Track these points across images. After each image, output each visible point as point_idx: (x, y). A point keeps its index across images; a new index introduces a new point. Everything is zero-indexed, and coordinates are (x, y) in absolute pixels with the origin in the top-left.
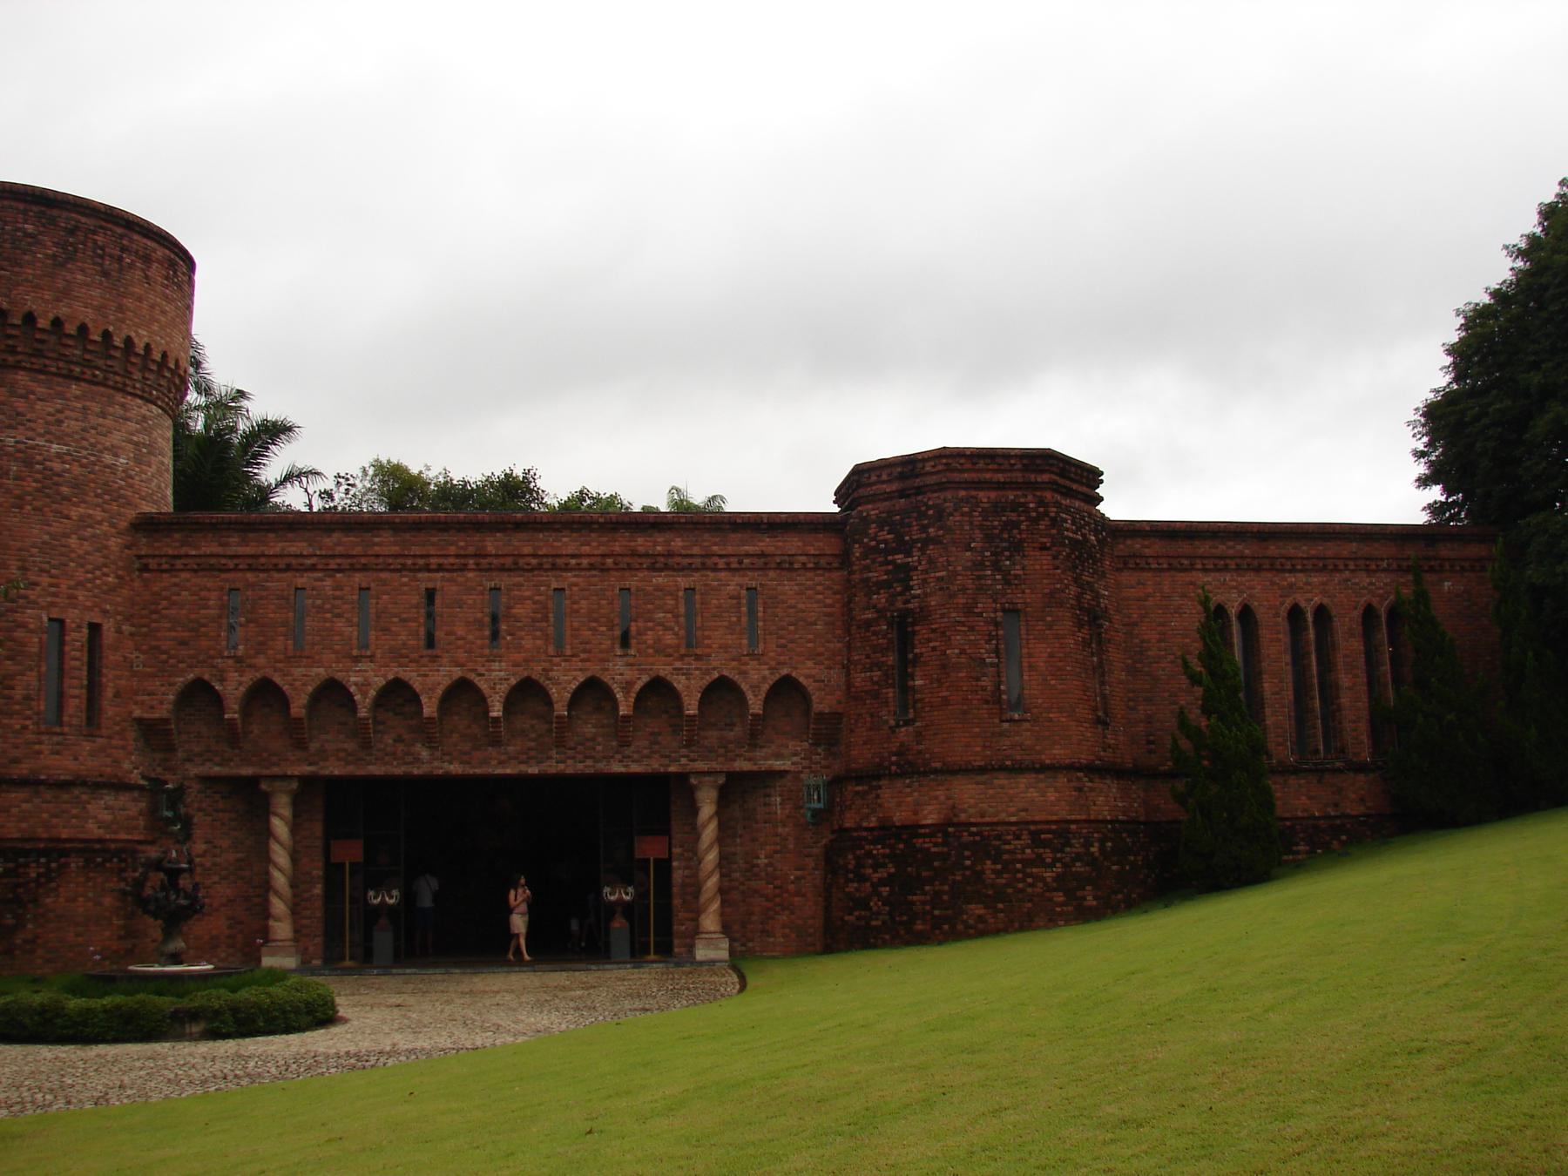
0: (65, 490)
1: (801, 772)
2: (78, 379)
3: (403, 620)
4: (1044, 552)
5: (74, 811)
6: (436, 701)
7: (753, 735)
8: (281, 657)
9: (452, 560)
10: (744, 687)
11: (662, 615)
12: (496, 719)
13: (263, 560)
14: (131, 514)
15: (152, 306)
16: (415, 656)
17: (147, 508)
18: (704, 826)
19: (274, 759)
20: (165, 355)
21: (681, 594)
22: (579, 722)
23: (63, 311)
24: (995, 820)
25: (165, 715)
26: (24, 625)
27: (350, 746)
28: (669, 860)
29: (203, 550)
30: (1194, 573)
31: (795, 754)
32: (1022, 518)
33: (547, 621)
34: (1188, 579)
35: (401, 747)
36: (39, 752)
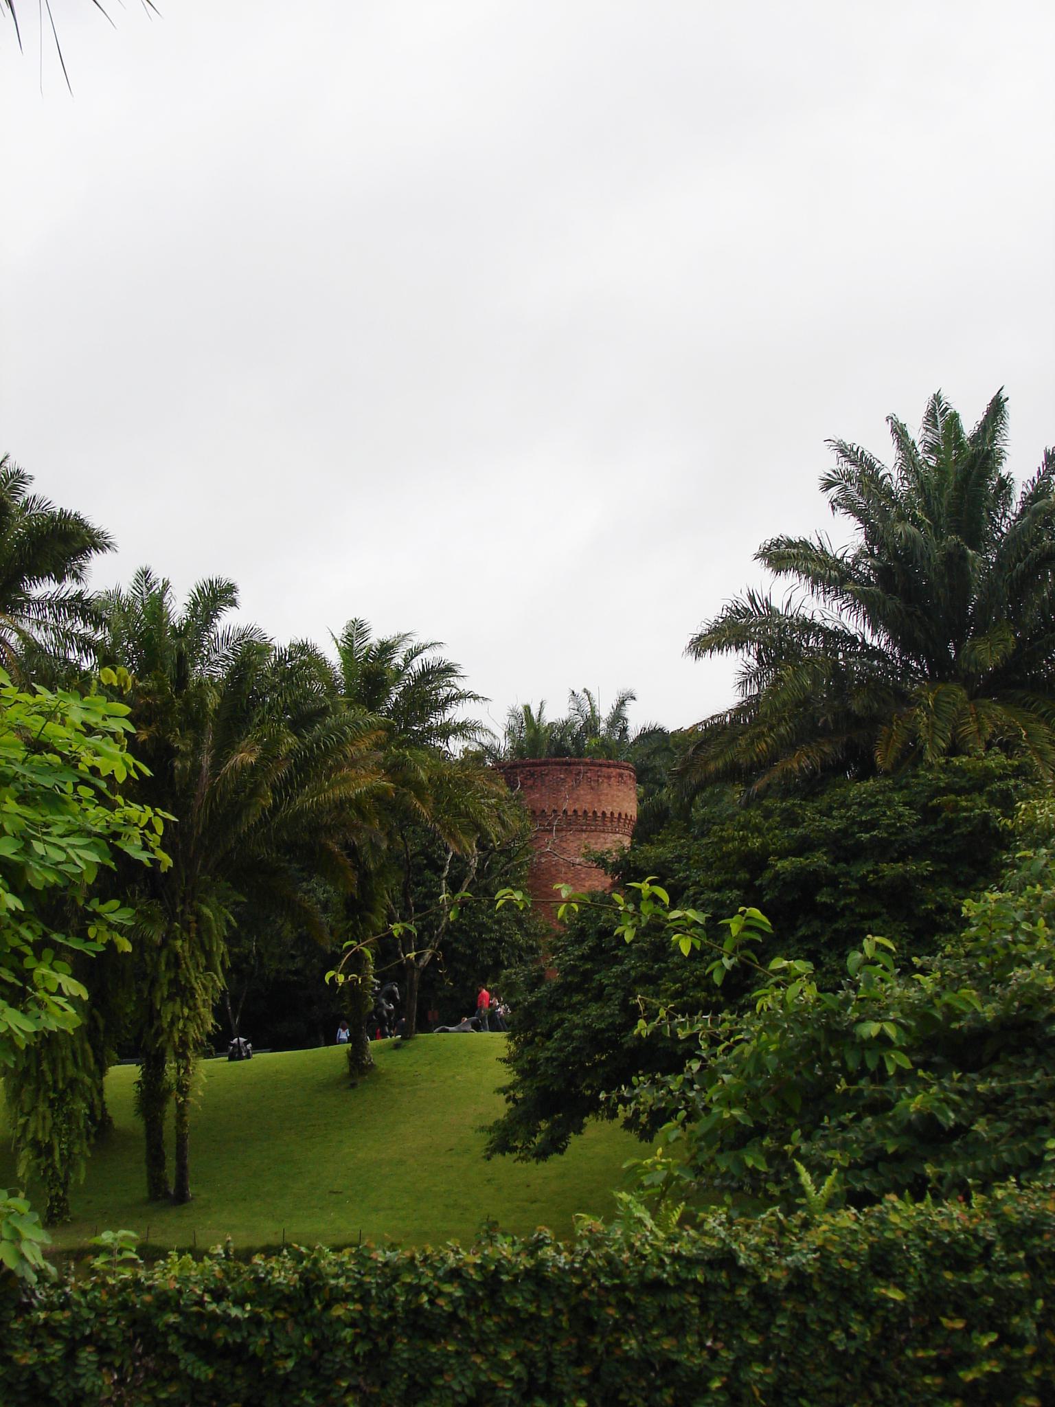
2: (585, 831)
15: (613, 796)
20: (620, 814)
23: (577, 807)
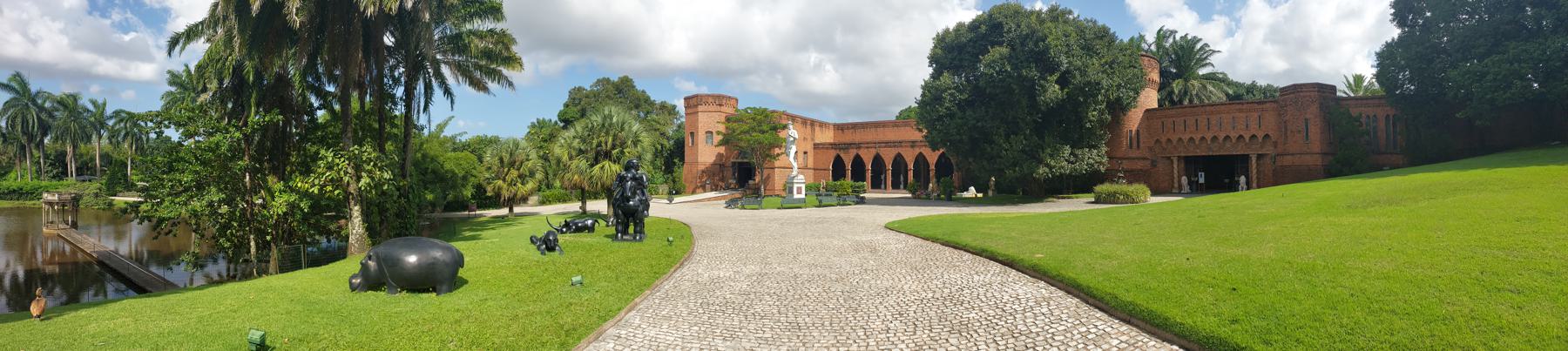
17: (1148, 108)
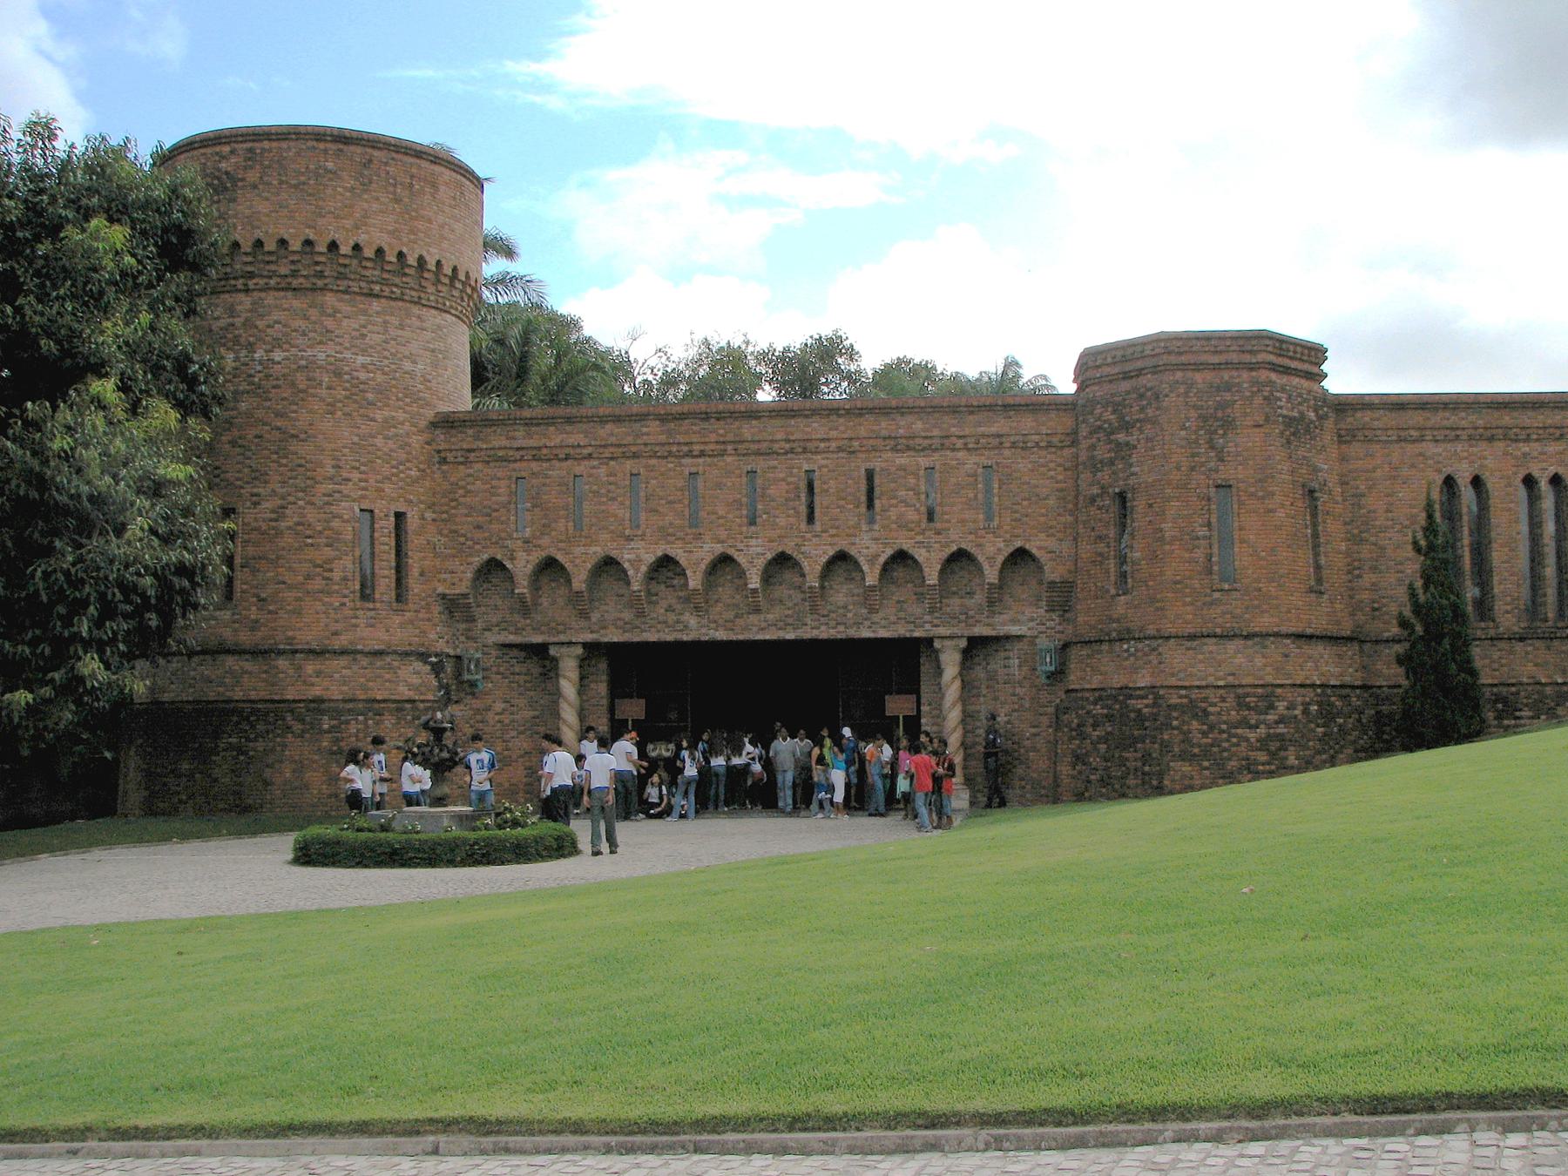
0: (370, 396)
1: (1036, 637)
2: (377, 296)
3: (670, 502)
4: (1257, 430)
5: (387, 676)
6: (700, 575)
7: (991, 603)
8: (563, 538)
9: (712, 447)
10: (979, 558)
11: (904, 493)
12: (755, 591)
13: (545, 451)
14: (429, 414)
15: (442, 226)
16: (680, 534)
17: (445, 408)
18: (948, 687)
19: (561, 628)
20: (455, 269)
21: (922, 472)
22: (832, 592)
23: (362, 238)
24: (1204, 683)
25: (464, 590)
26: (339, 517)
27: (627, 615)
28: (918, 716)
29: (496, 444)
30: (1424, 444)
31: (1032, 620)
32: (1236, 398)
33: (800, 500)
34: (1417, 451)
35: (672, 617)
36: (356, 626)
